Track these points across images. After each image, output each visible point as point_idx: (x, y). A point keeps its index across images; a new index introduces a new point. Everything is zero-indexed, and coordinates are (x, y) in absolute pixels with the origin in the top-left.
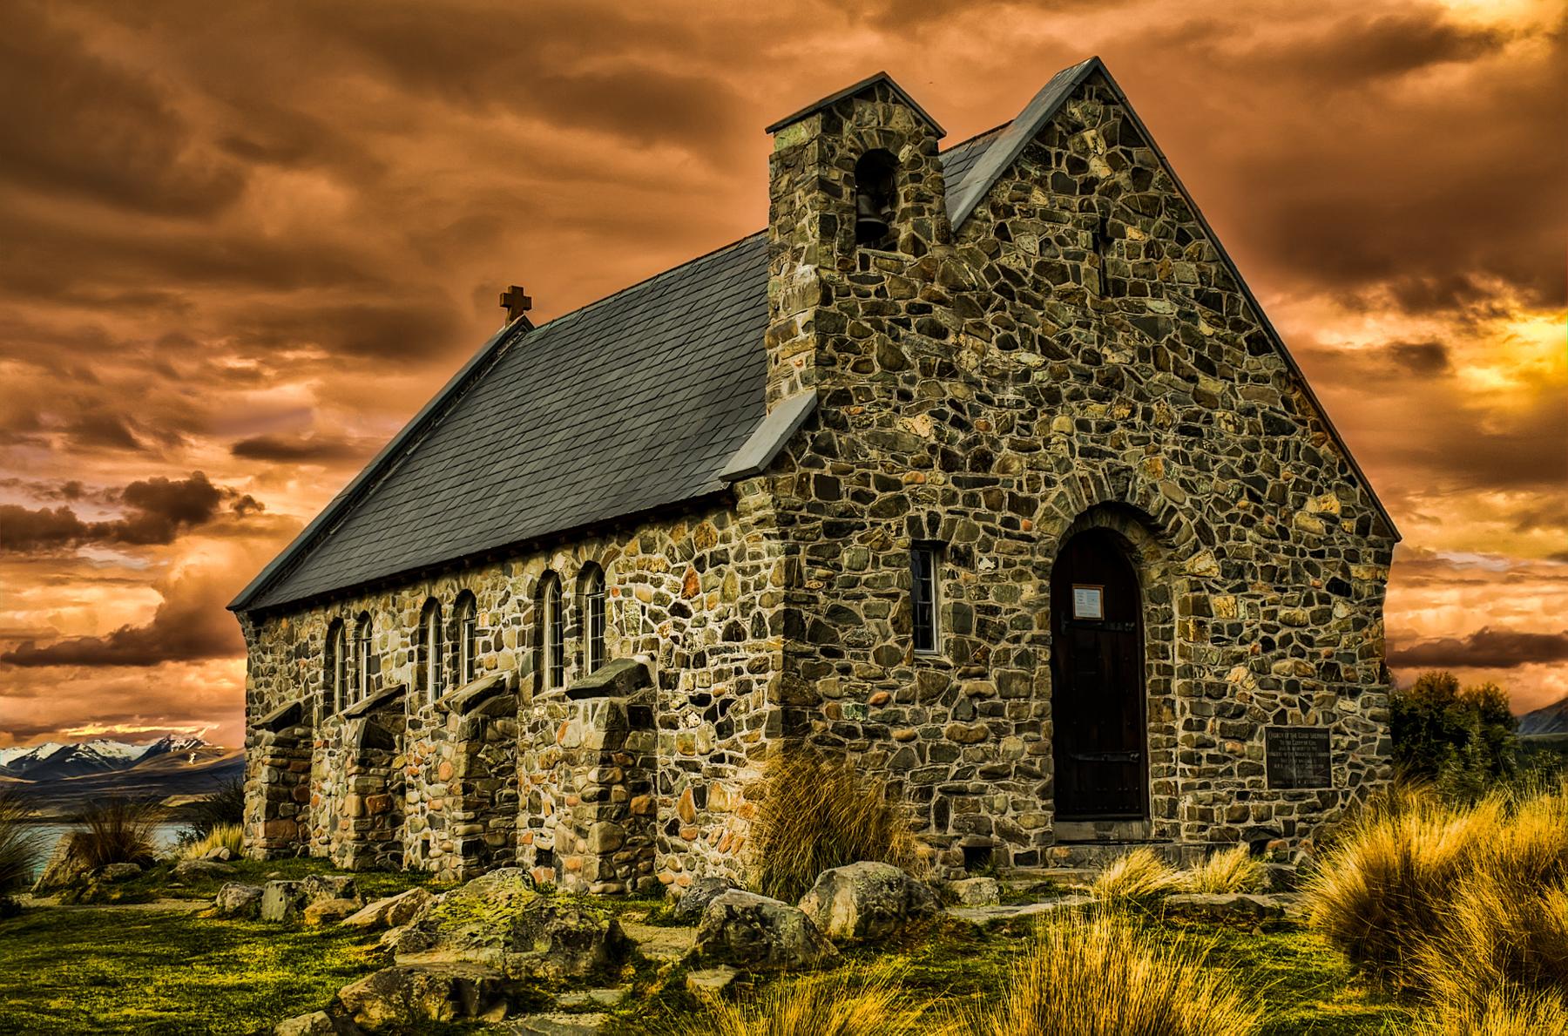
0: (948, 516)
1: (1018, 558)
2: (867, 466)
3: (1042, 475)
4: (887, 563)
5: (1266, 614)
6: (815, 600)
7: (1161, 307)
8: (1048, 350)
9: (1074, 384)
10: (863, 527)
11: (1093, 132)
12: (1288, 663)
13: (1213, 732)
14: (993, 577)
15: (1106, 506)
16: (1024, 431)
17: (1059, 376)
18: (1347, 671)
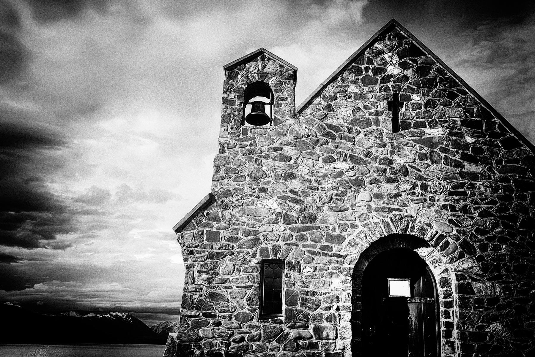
0: (286, 246)
3: (349, 223)
4: (245, 271)
10: (233, 254)
11: (390, 54)
14: (312, 276)
16: (338, 202)
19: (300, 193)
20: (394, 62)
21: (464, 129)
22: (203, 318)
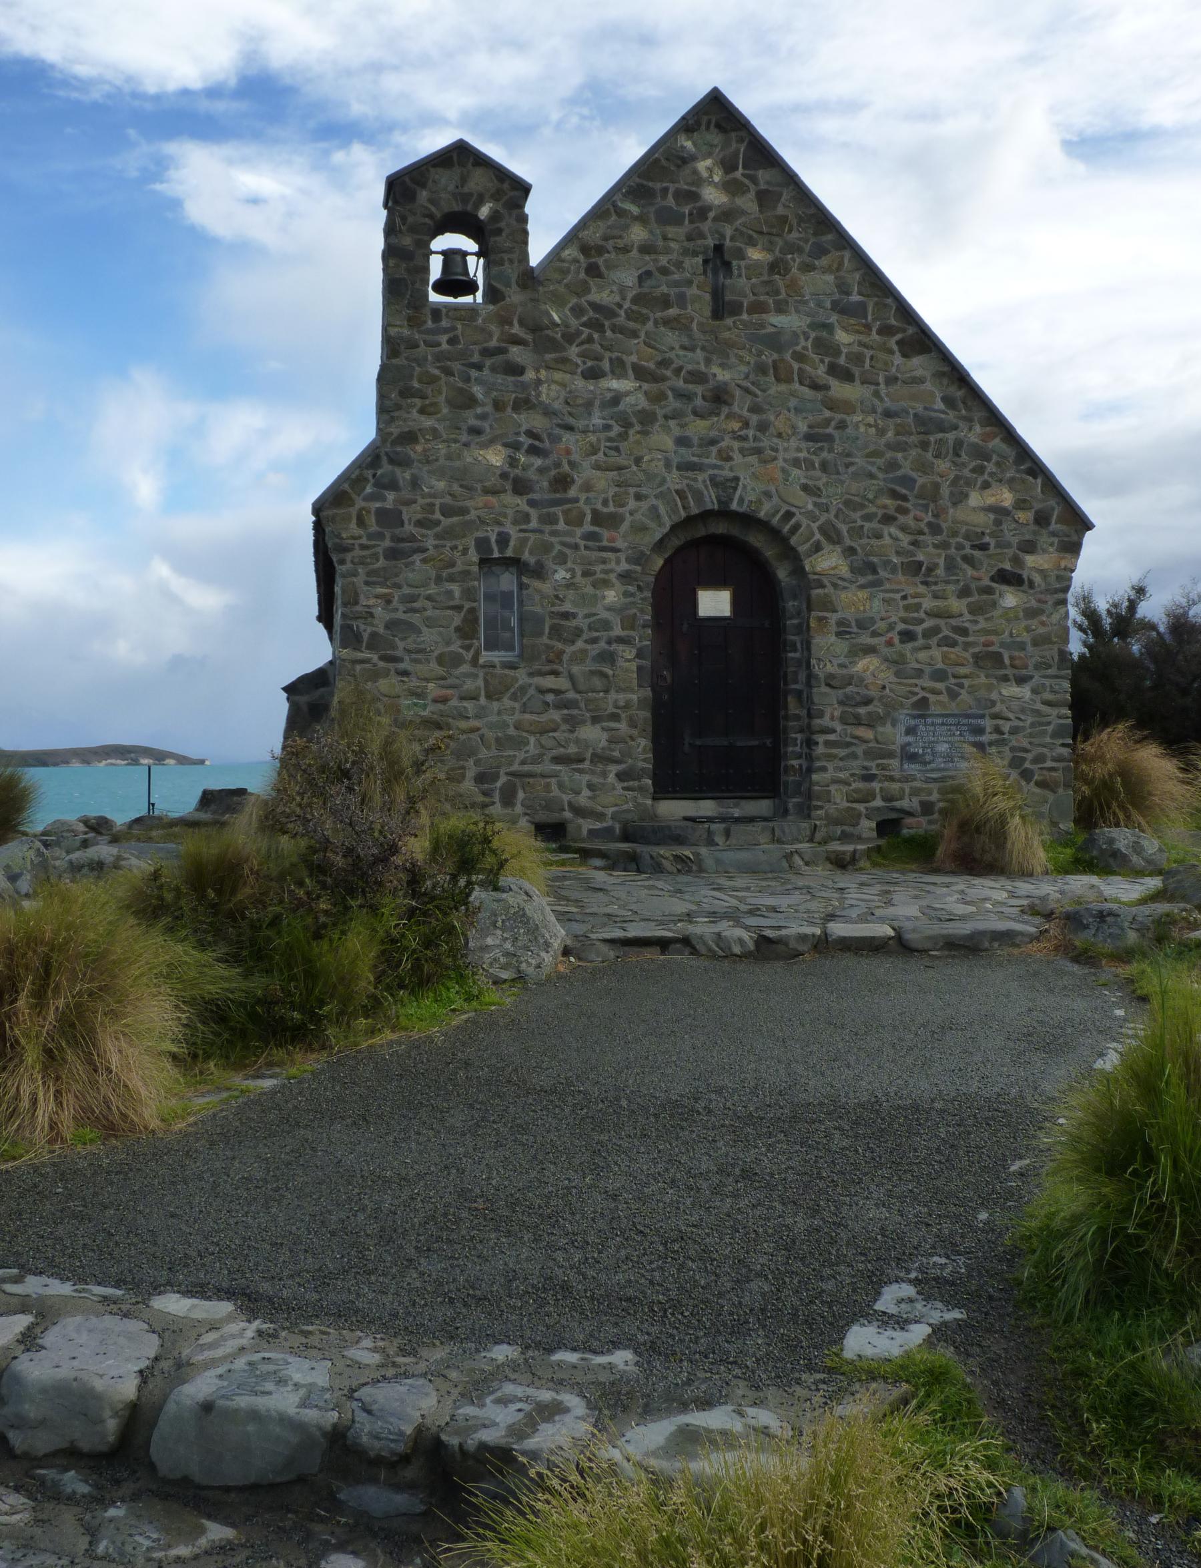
0: (522, 535)
1: (598, 568)
2: (434, 496)
4: (451, 579)
5: (907, 608)
6: (371, 615)
7: (789, 322)
8: (641, 374)
9: (673, 403)
10: (425, 550)
11: (709, 162)
12: (937, 653)
13: (832, 718)
14: (570, 585)
15: (706, 515)
16: (613, 453)
17: (659, 398)
18: (1012, 658)
19: (545, 436)
20: (716, 179)
21: (834, 318)
22: (382, 664)
